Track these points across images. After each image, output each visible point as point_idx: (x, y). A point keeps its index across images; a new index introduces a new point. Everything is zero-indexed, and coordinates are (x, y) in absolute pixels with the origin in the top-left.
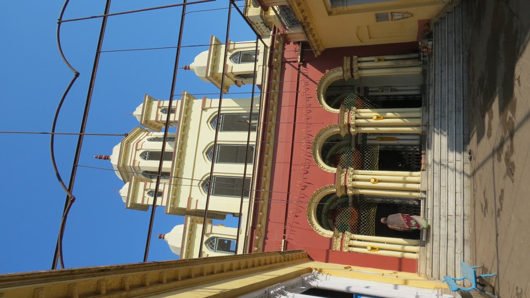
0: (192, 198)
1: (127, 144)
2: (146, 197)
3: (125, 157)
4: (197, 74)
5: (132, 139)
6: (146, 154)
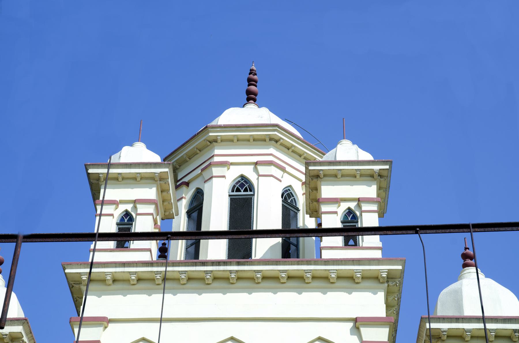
0: (106, 328)
1: (271, 139)
2: (116, 209)
3: (235, 140)
4: (445, 291)
5: (288, 149)
6: (246, 190)
